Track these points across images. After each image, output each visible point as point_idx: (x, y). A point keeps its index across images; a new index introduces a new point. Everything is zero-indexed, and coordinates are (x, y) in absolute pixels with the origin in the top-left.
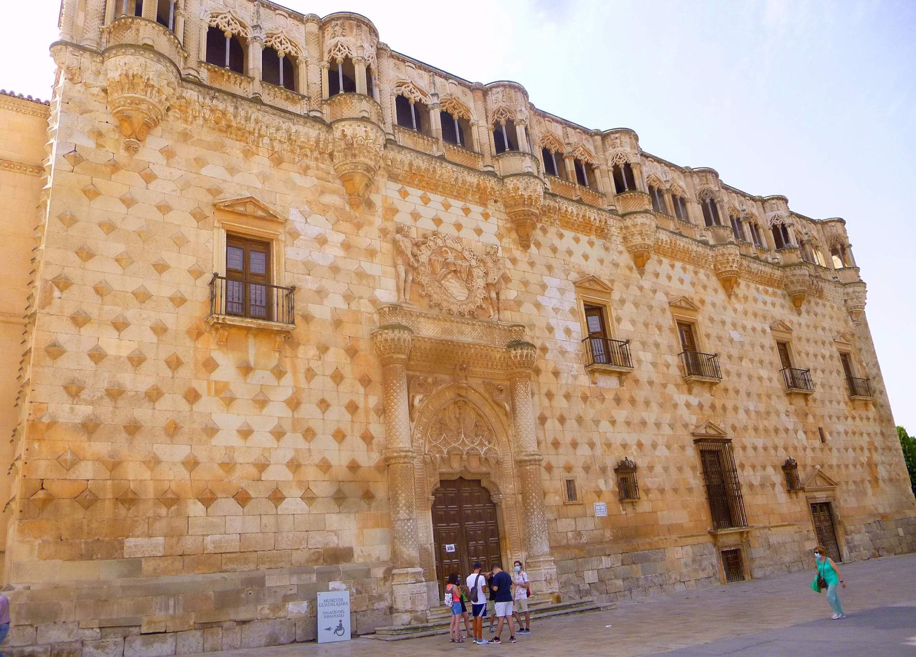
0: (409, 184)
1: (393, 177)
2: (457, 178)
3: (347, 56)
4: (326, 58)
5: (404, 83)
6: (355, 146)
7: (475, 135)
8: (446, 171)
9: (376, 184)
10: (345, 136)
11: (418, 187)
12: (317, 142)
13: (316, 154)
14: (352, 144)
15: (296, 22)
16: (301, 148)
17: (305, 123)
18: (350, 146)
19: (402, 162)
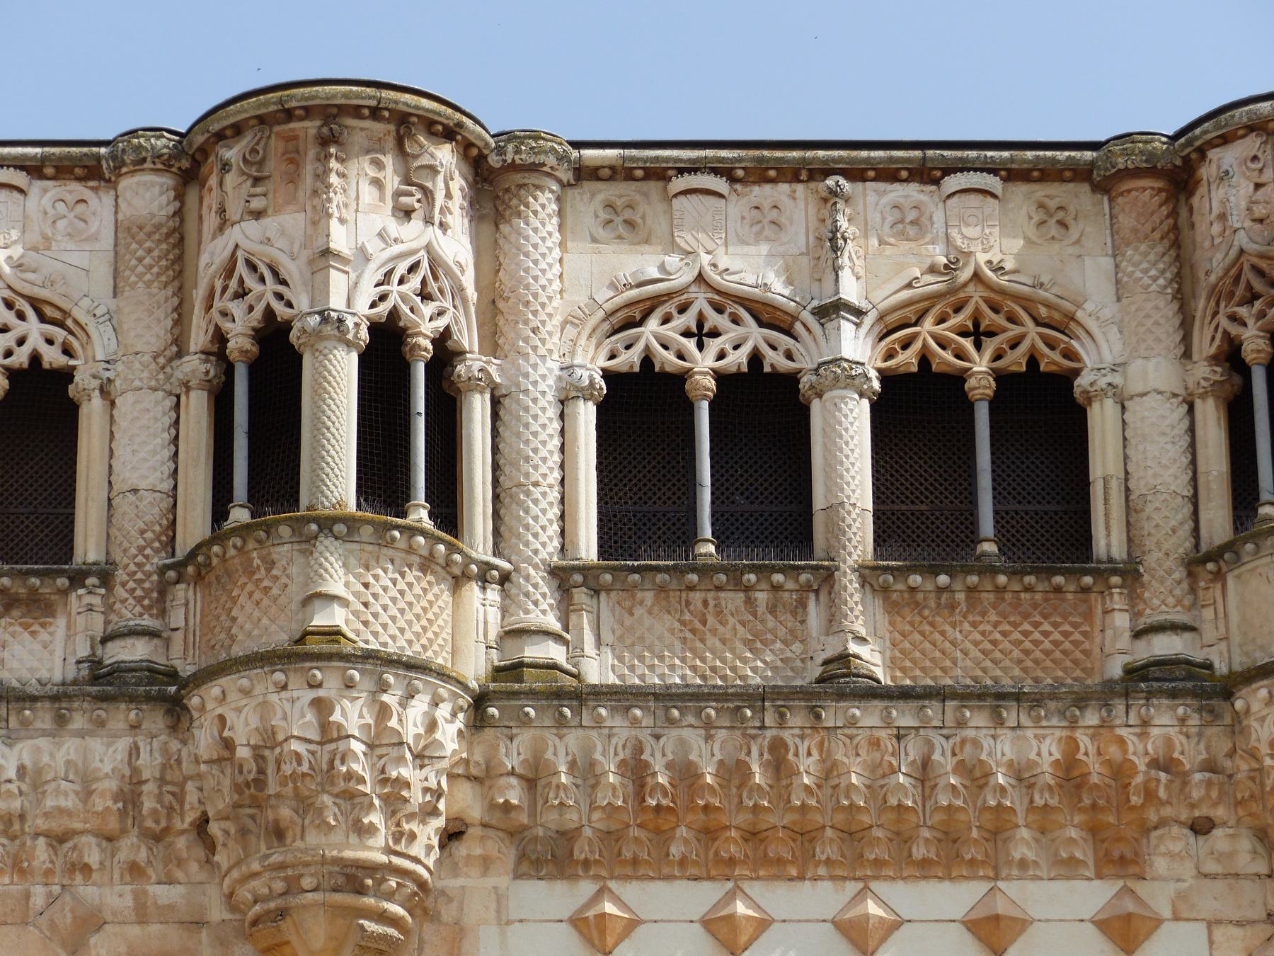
0: (634, 869)
1: (547, 856)
2: (924, 773)
3: (269, 313)
4: (199, 338)
5: (648, 307)
6: (272, 788)
7: (1103, 458)
8: (853, 757)
9: (448, 913)
10: (229, 745)
11: (687, 870)
12: (129, 797)
13: (131, 848)
14: (260, 783)
15: (75, 189)
16: (58, 839)
17: (61, 720)
18: (253, 791)
19: (587, 772)
